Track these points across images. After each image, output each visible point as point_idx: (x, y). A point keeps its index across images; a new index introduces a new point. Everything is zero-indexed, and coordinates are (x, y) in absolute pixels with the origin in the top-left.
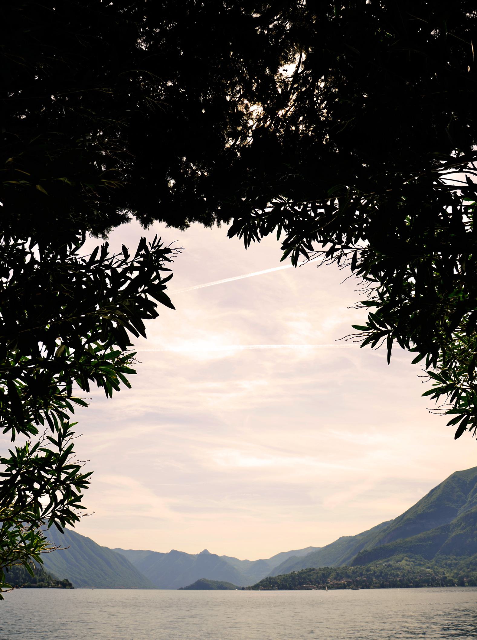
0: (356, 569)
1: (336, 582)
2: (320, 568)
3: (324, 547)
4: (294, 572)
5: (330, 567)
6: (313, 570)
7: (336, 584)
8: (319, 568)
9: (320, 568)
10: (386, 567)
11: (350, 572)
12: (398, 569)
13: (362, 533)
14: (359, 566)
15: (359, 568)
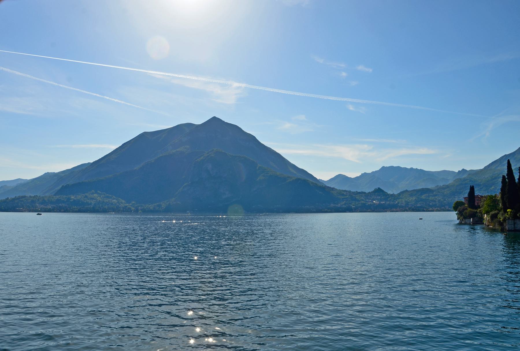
0: (60, 197)
1: (43, 207)
2: (30, 196)
3: (31, 179)
4: (8, 198)
5: (38, 196)
6: (25, 197)
7: (44, 208)
8: (29, 196)
9: (30, 196)
10: (83, 197)
11: (55, 200)
12: (92, 199)
13: (64, 171)
14: (62, 196)
15: (62, 197)
